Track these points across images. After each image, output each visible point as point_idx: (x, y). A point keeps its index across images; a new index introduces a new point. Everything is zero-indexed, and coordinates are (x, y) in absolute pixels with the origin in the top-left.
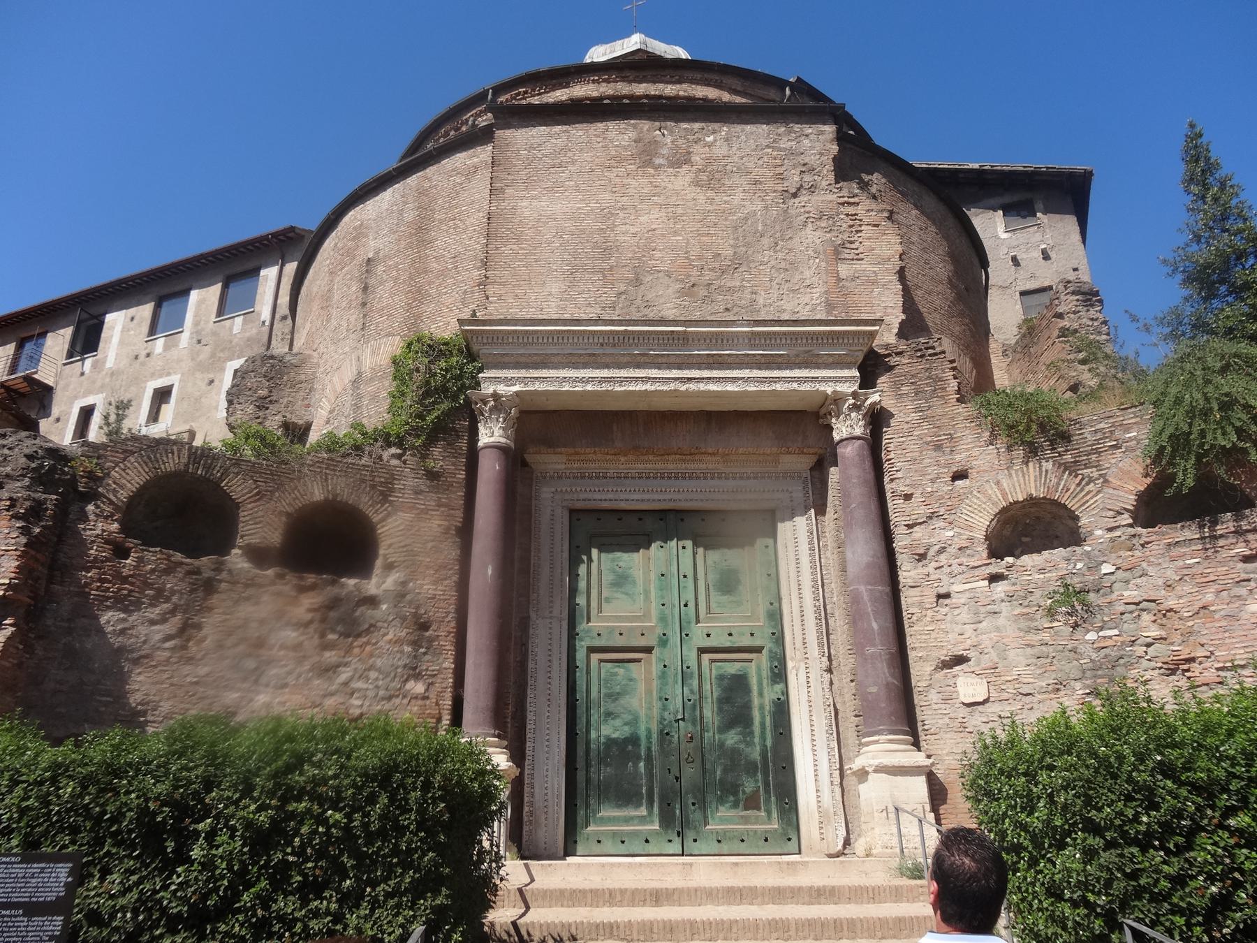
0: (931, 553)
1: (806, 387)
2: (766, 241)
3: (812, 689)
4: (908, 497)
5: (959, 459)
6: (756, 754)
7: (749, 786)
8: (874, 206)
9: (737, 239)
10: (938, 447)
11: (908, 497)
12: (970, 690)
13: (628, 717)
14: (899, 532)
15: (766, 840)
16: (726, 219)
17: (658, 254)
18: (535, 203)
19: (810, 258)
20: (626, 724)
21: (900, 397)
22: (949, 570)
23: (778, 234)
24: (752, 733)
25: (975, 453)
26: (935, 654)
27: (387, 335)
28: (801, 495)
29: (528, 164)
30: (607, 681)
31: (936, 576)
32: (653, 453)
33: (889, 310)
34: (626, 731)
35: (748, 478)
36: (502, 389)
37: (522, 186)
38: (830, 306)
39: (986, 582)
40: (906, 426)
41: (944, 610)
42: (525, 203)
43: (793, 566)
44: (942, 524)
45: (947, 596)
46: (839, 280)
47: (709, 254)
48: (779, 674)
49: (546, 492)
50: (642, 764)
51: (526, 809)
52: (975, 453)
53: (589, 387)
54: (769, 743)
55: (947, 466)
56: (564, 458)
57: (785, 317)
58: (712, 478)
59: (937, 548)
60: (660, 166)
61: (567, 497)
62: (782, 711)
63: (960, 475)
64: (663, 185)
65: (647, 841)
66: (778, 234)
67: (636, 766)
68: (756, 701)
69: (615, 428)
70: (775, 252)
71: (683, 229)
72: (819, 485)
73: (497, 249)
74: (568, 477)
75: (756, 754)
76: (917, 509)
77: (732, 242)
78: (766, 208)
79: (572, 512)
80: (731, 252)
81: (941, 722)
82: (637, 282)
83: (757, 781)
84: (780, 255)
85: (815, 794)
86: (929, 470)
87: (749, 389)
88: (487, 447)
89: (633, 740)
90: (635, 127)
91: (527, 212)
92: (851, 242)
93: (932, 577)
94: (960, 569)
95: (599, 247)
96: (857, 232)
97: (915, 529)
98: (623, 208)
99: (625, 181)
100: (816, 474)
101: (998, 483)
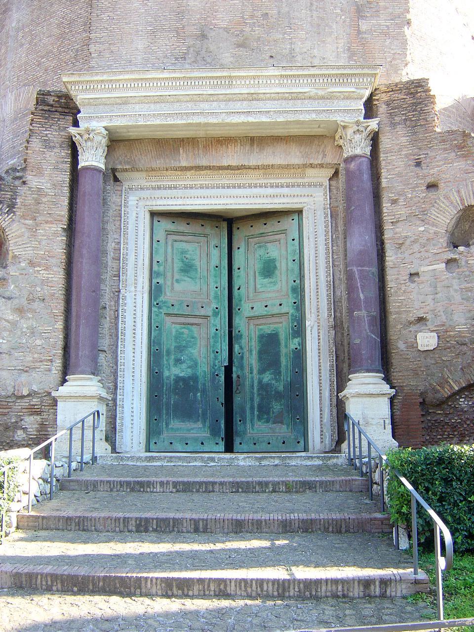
0: (408, 242)
1: (322, 117)
3: (321, 340)
4: (394, 202)
5: (432, 172)
6: (281, 388)
7: (277, 407)
10: (418, 164)
11: (394, 202)
12: (425, 342)
13: (190, 363)
14: (387, 227)
15: (284, 443)
19: (337, 15)
20: (189, 367)
21: (393, 125)
22: (418, 255)
24: (280, 372)
25: (444, 168)
27: (25, 85)
30: (176, 338)
31: (411, 260)
32: (210, 169)
33: (397, 56)
34: (189, 372)
35: (282, 186)
38: (352, 54)
39: (443, 266)
41: (413, 286)
43: (313, 252)
44: (418, 222)
45: (417, 274)
46: (359, 32)
47: (259, 14)
48: (299, 330)
49: (132, 200)
50: (199, 394)
51: (118, 421)
52: (444, 168)
53: (158, 122)
54: (289, 380)
55: (424, 177)
56: (144, 174)
57: (316, 62)
58: (256, 187)
59: (412, 239)
62: (299, 356)
63: (432, 186)
65: (202, 443)
67: (195, 395)
68: (283, 351)
69: (181, 151)
70: (311, 10)
72: (335, 192)
73: (97, 16)
74: (148, 189)
75: (281, 388)
76: (401, 211)
79: (153, 214)
82: (203, 36)
83: (281, 405)
84: (315, 14)
85: (319, 413)
88: (86, 168)
89: (194, 378)
94: (426, 255)
95: (174, 11)
97: (399, 225)
100: (333, 183)
101: (459, 191)
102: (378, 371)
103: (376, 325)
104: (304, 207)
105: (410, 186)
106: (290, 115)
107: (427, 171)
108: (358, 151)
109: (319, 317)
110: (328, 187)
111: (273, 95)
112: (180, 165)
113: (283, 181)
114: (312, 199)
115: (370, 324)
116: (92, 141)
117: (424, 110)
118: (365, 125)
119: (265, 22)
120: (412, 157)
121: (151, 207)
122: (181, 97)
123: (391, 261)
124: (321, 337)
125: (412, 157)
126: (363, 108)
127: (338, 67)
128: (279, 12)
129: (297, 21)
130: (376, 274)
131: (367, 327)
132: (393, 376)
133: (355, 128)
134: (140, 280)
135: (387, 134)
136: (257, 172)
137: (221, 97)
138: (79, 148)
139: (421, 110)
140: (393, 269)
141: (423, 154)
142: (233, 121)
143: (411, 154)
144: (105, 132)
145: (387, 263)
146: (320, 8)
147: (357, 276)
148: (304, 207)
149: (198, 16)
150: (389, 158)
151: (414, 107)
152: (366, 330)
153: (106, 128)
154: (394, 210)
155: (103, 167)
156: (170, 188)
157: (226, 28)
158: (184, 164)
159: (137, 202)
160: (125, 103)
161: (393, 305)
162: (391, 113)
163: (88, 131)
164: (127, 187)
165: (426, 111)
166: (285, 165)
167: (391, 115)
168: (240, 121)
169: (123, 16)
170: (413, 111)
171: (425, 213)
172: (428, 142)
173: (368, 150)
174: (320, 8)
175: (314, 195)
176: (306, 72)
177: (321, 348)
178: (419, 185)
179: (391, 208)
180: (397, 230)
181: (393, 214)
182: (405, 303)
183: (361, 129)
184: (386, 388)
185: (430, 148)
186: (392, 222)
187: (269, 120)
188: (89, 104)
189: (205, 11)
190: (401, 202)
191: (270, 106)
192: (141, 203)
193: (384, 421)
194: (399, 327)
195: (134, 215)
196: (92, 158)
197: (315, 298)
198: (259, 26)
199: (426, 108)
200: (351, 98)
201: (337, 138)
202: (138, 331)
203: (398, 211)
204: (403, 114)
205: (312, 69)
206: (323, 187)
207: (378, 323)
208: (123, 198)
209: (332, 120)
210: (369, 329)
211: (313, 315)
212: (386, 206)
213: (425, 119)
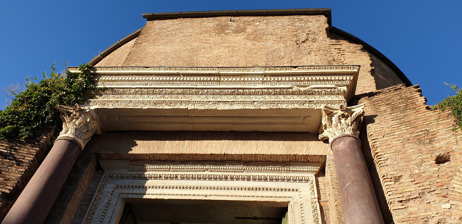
29: (158, 34)
42: (151, 47)
49: (109, 187)
60: (228, 33)
61: (125, 191)
71: (237, 55)
74: (128, 178)
87: (262, 108)
90: (218, 20)
97: (411, 203)
100: (320, 179)
104: (289, 202)
105: (414, 162)
110: (314, 181)
113: (266, 174)
114: (297, 193)
121: (126, 195)
148: (289, 202)
159: (113, 189)
164: (108, 175)
165: (414, 97)
170: (399, 100)
176: (288, 71)
185: (428, 125)
186: (401, 202)
195: (106, 200)
203: (404, 189)
204: (387, 104)
205: (293, 69)
206: (310, 182)
208: (100, 184)
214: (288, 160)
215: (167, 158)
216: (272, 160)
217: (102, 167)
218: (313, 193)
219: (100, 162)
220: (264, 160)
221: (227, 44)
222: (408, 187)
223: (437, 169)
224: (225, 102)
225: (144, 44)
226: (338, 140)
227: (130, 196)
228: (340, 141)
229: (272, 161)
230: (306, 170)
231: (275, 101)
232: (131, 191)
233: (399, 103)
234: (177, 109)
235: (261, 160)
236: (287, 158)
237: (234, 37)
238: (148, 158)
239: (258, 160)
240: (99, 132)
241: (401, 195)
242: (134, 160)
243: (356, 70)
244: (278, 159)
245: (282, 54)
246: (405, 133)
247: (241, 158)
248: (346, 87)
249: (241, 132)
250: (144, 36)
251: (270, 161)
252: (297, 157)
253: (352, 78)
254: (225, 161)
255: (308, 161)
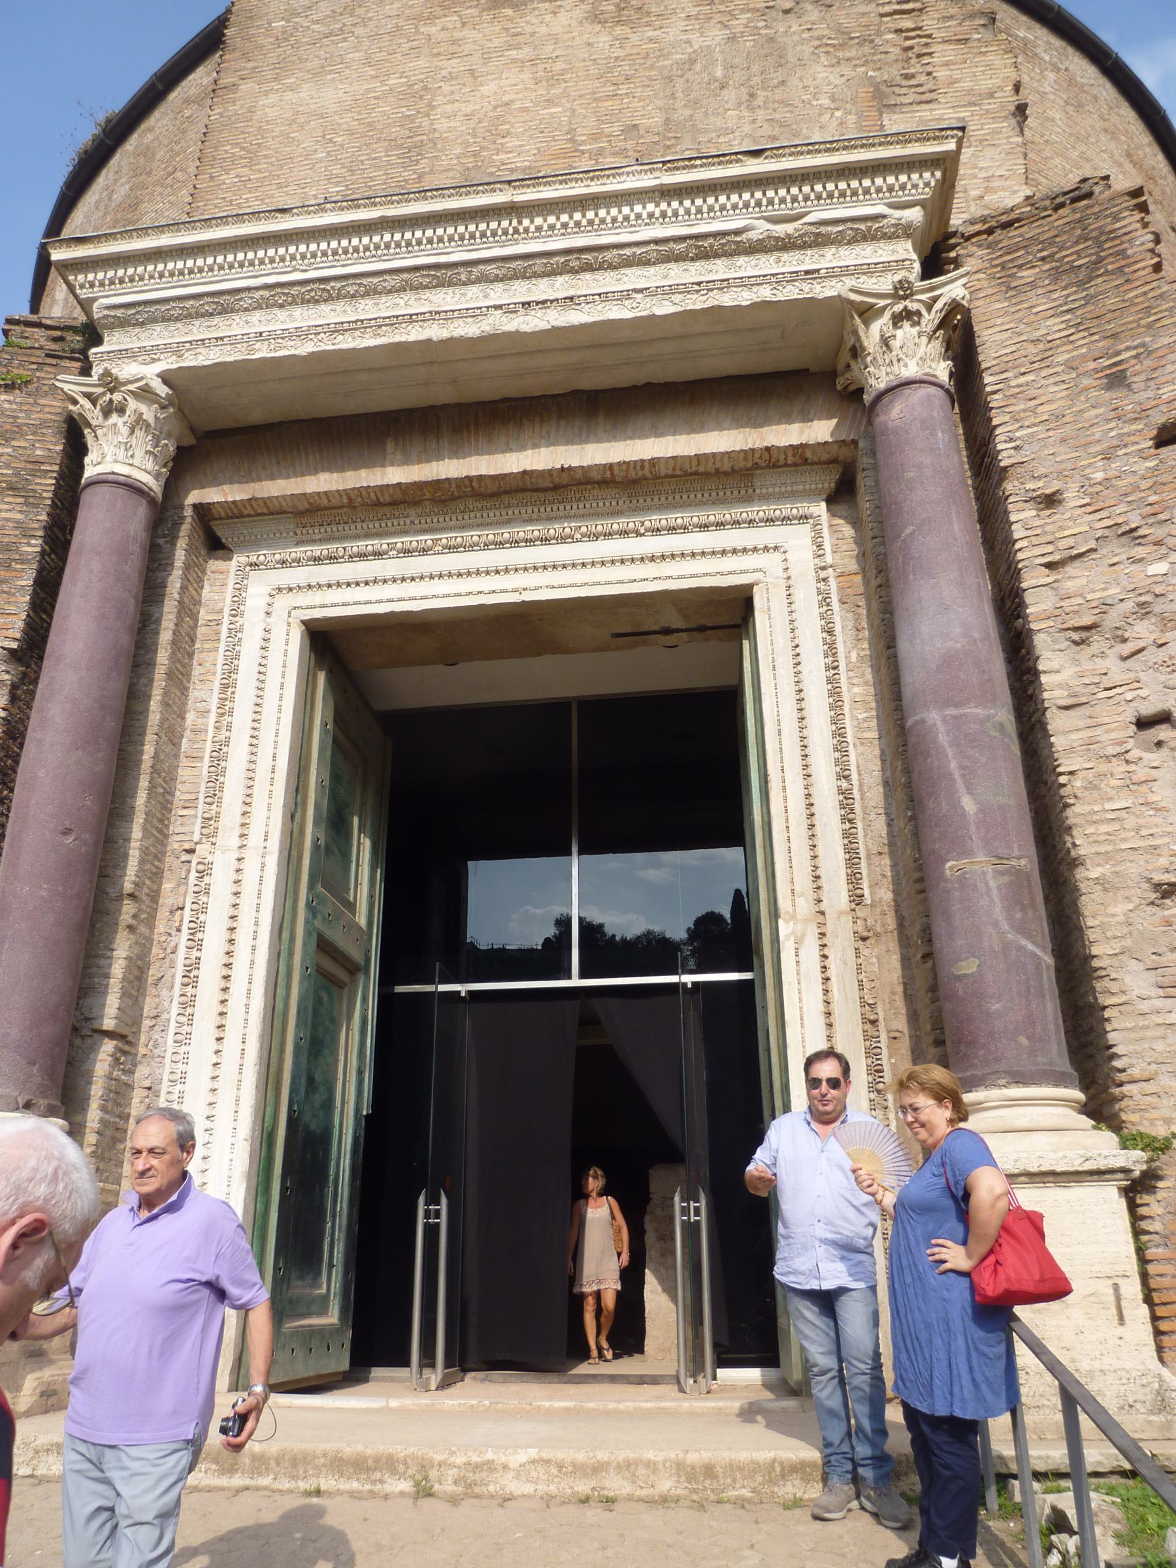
0: (1113, 618)
1: (790, 292)
2: (730, 95)
3: (834, 984)
4: (1050, 501)
8: (953, 11)
9: (673, 96)
10: (1117, 379)
11: (1050, 501)
14: (1032, 579)
16: (652, 67)
17: (511, 142)
18: (289, 96)
19: (823, 109)
23: (756, 80)
26: (1134, 869)
28: (809, 554)
29: (285, 37)
31: (1131, 676)
36: (126, 370)
37: (269, 75)
40: (1032, 349)
41: (1154, 758)
42: (272, 99)
44: (1140, 552)
47: (616, 129)
53: (306, 348)
55: (1142, 413)
59: (1129, 605)
64: (528, 29)
66: (756, 80)
69: (390, 446)
71: (565, 94)
73: (212, 178)
76: (1073, 524)
77: (659, 103)
78: (732, 39)
80: (656, 120)
81: (1160, 1046)
84: (761, 114)
86: (1097, 432)
87: (659, 311)
91: (272, 113)
92: (907, 77)
93: (1116, 677)
95: (401, 147)
96: (920, 56)
97: (1070, 569)
98: (451, 77)
99: (458, 35)
102: (1059, 1080)
103: (1033, 905)
106: (695, 296)
107: (1150, 394)
108: (911, 370)
109: (823, 906)
111: (639, 251)
112: (385, 482)
114: (776, 557)
115: (1014, 898)
116: (121, 410)
117: (1111, 232)
118: (924, 297)
119: (630, 145)
120: (1092, 365)
122: (376, 280)
123: (1060, 686)
124: (832, 972)
125: (1092, 365)
126: (914, 257)
127: (830, 146)
128: (668, 119)
129: (714, 135)
130: (1011, 727)
131: (998, 912)
132: (1124, 1097)
133: (898, 308)
134: (259, 813)
135: (999, 321)
136: (610, 492)
137: (490, 268)
138: (86, 431)
139: (1102, 233)
140: (1072, 713)
141: (1128, 349)
142: (525, 328)
143: (1084, 357)
144: (163, 390)
145: (1046, 695)
146: (774, 102)
147: (943, 738)
149: (459, 151)
150: (1013, 383)
151: (1079, 232)
152: (996, 924)
153: (165, 378)
154: (1049, 528)
155: (155, 486)
156: (363, 556)
157: (530, 167)
158: (396, 474)
160: (225, 311)
161: (1088, 834)
162: (1003, 266)
163: (111, 383)
165: (1124, 230)
166: (690, 457)
167: (1003, 268)
168: (545, 326)
169: (271, 172)
170: (1077, 243)
171: (1163, 517)
172: (1139, 312)
173: (943, 370)
174: (774, 102)
175: (786, 547)
177: (835, 1008)
178: (1126, 439)
179: (1038, 523)
180: (1069, 584)
181: (1049, 538)
182: (1131, 822)
183: (913, 306)
184: (1103, 1148)
185: (1149, 326)
186: (1050, 566)
187: (628, 315)
188: (122, 323)
189: (475, 136)
190: (1072, 497)
191: (633, 278)
192: (284, 602)
193: (1116, 1287)
194: (1120, 909)
195: (260, 634)
196: (122, 454)
197: (806, 844)
198: (614, 154)
199: (1118, 225)
200: (874, 238)
201: (840, 366)
202: (240, 972)
204: (1043, 259)
205: (752, 161)
207: (1040, 899)
209: (822, 296)
210: (1010, 919)
211: (800, 901)
212: (1022, 518)
213: (1122, 254)
214: (750, 465)
215: (399, 496)
216: (701, 469)
217: (223, 540)
218: (821, 552)
219: (215, 528)
220: (678, 472)
221: (525, 53)
222: (1073, 524)
223: (1151, 464)
224: (544, 302)
225: (245, 87)
226: (886, 399)
227: (318, 614)
228: (891, 401)
229: (702, 474)
230: (801, 487)
231: (699, 284)
232: (316, 597)
233: (1077, 252)
234: (400, 343)
235: (670, 472)
236: (745, 459)
237: (548, 18)
238: (345, 500)
239: (663, 472)
240: (190, 440)
241: (1050, 548)
242: (308, 511)
243: (951, 146)
244: (718, 465)
245: (719, 72)
246: (1083, 356)
247: (612, 474)
248: (918, 208)
249: (604, 391)
250: (238, 54)
251: (696, 473)
252: (774, 453)
253: (938, 174)
254: (565, 486)
255: (805, 461)
